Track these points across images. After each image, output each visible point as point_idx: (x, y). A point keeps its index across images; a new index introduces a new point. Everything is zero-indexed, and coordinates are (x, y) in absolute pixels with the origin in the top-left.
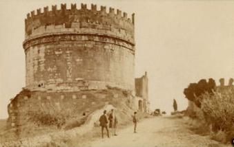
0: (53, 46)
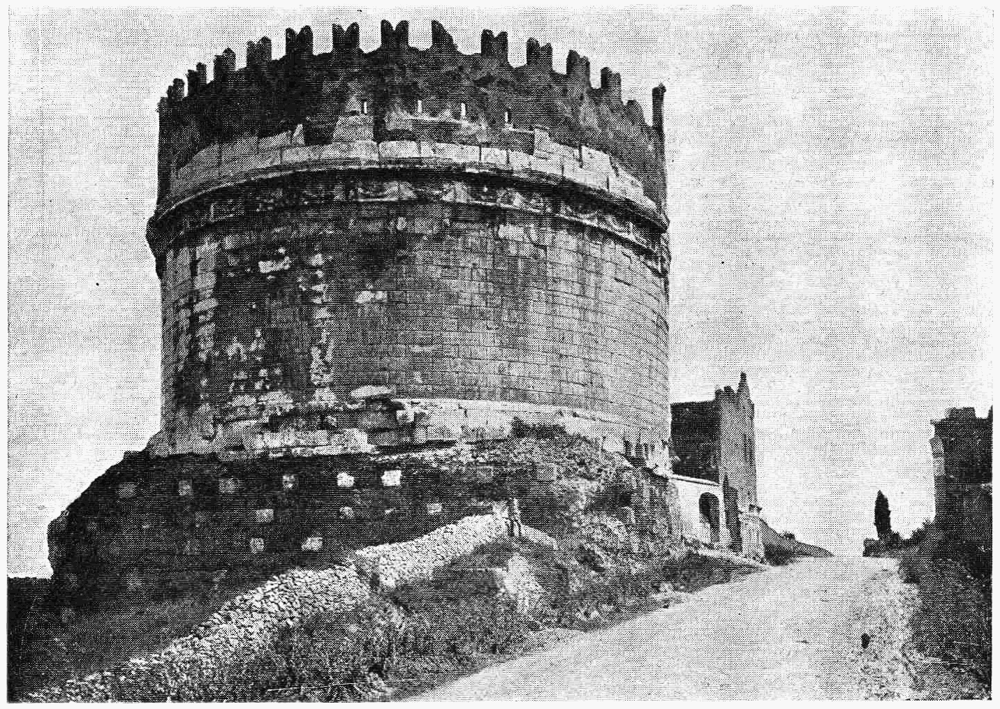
0: (249, 238)
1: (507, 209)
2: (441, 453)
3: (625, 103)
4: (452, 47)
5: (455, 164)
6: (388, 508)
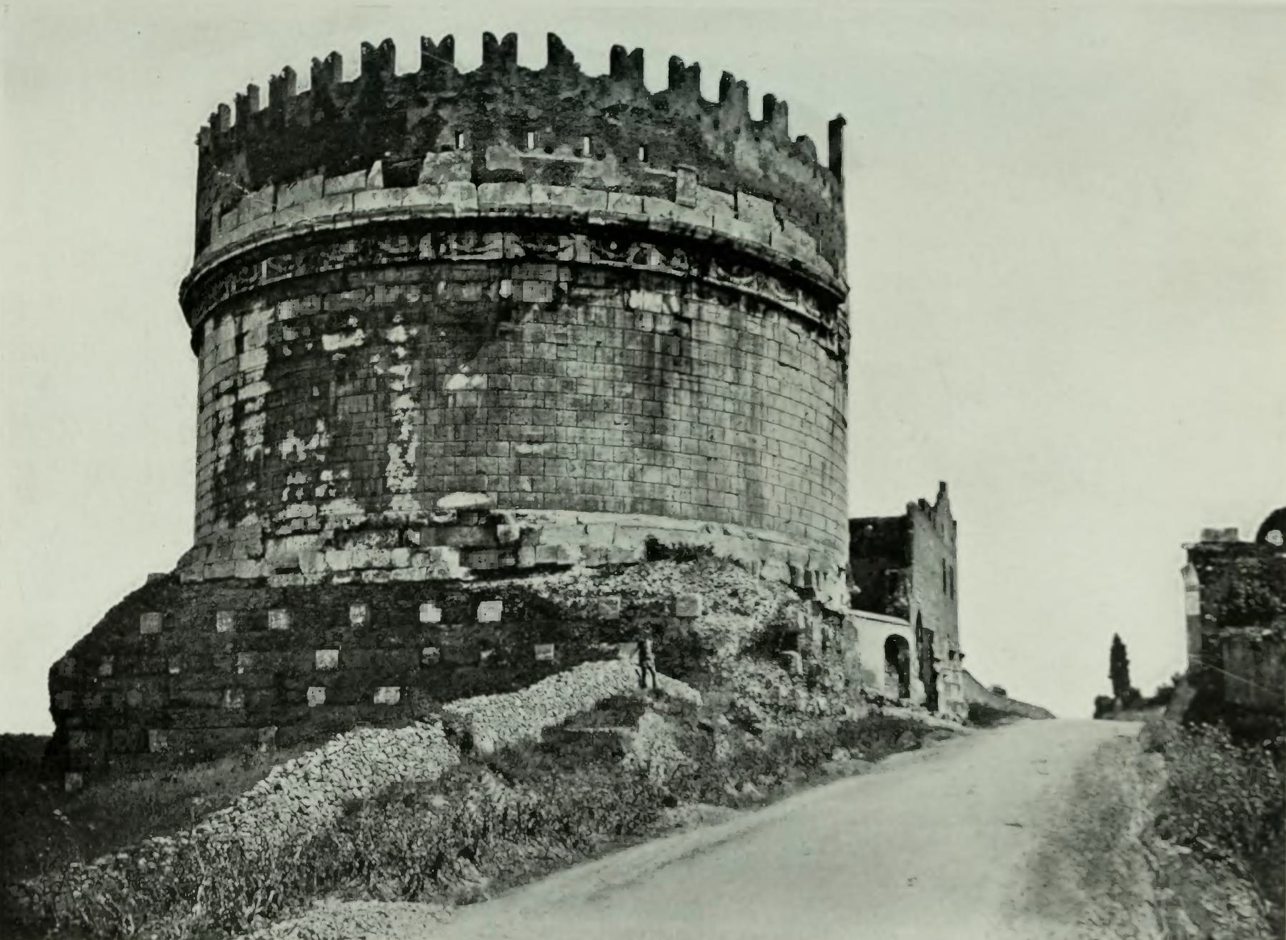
0: (311, 303)
1: (639, 271)
2: (554, 579)
3: (794, 140)
4: (573, 69)
5: (576, 213)
6: (484, 650)
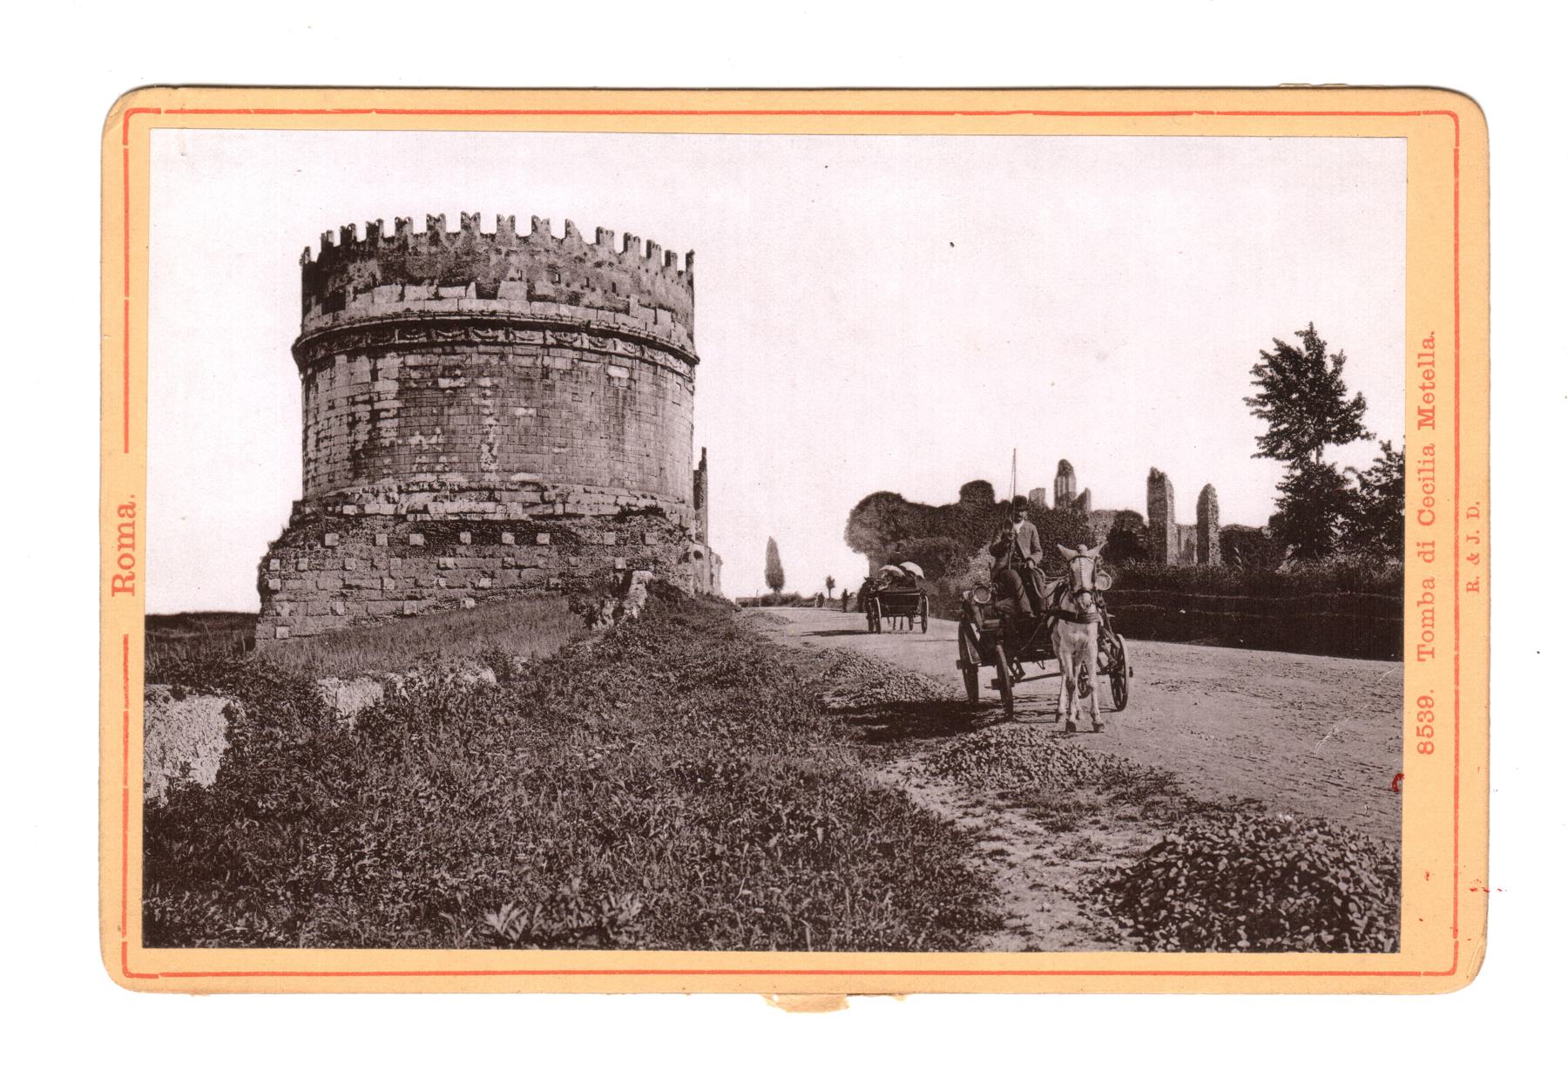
2: (576, 521)
